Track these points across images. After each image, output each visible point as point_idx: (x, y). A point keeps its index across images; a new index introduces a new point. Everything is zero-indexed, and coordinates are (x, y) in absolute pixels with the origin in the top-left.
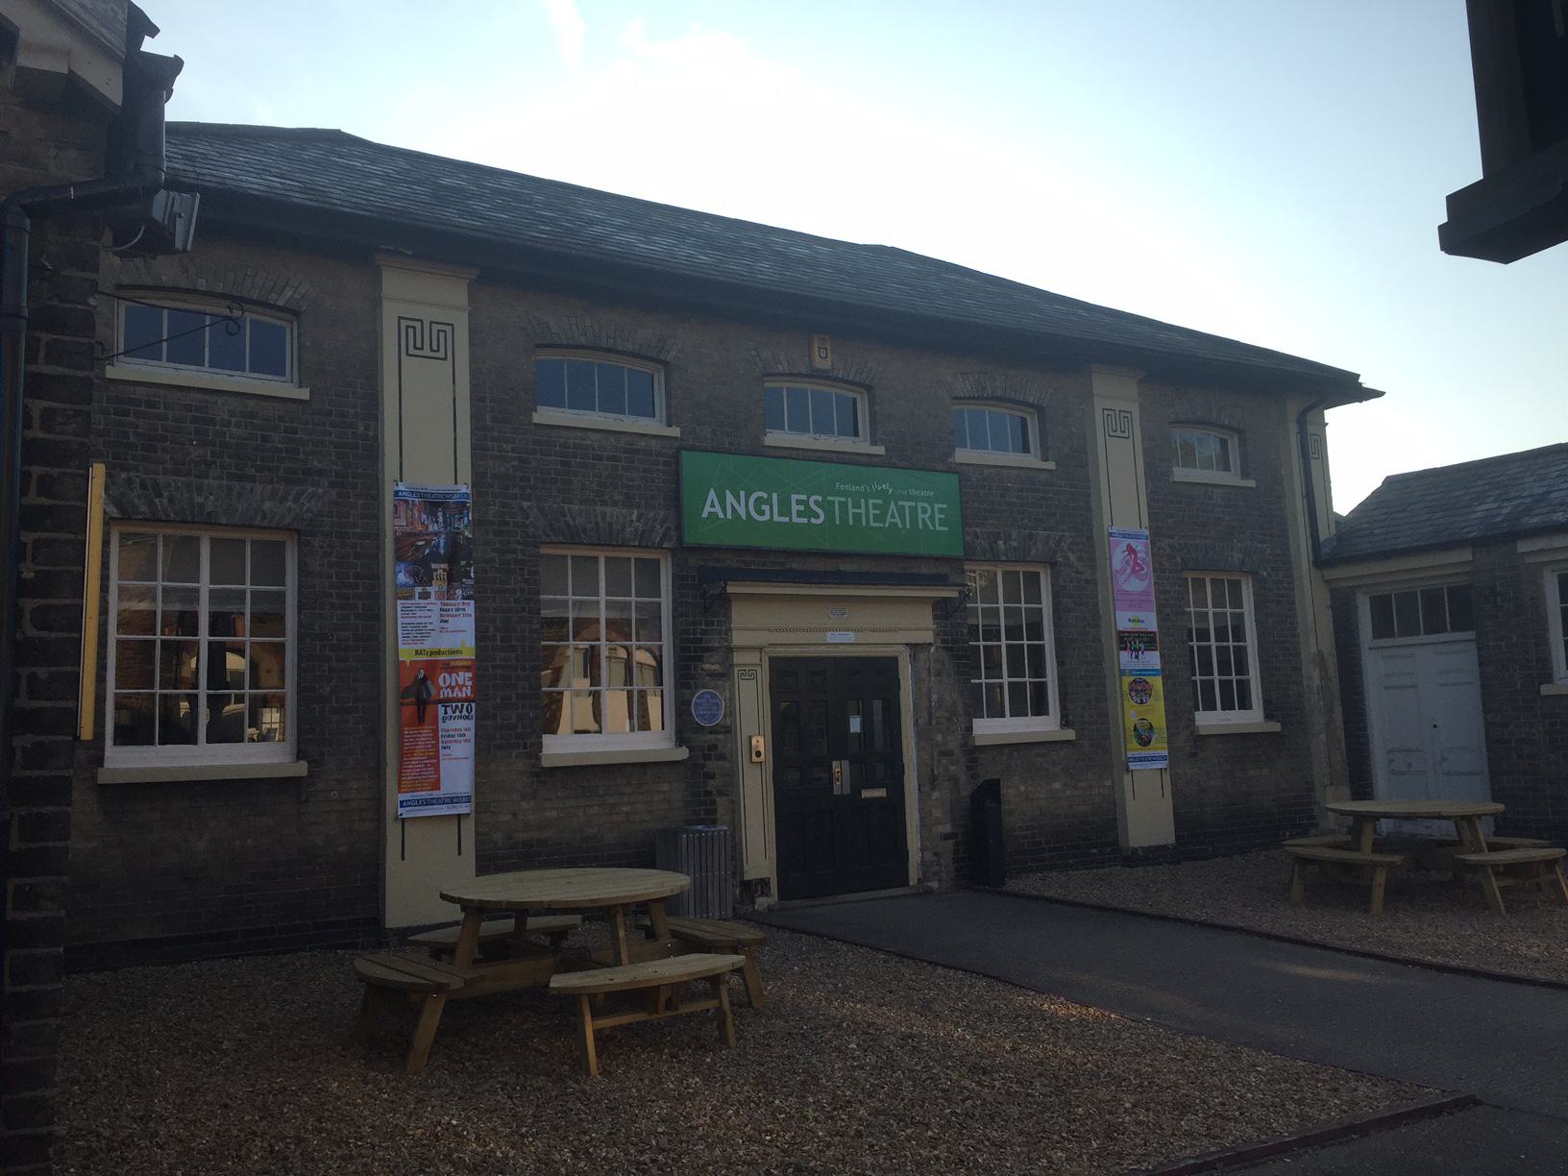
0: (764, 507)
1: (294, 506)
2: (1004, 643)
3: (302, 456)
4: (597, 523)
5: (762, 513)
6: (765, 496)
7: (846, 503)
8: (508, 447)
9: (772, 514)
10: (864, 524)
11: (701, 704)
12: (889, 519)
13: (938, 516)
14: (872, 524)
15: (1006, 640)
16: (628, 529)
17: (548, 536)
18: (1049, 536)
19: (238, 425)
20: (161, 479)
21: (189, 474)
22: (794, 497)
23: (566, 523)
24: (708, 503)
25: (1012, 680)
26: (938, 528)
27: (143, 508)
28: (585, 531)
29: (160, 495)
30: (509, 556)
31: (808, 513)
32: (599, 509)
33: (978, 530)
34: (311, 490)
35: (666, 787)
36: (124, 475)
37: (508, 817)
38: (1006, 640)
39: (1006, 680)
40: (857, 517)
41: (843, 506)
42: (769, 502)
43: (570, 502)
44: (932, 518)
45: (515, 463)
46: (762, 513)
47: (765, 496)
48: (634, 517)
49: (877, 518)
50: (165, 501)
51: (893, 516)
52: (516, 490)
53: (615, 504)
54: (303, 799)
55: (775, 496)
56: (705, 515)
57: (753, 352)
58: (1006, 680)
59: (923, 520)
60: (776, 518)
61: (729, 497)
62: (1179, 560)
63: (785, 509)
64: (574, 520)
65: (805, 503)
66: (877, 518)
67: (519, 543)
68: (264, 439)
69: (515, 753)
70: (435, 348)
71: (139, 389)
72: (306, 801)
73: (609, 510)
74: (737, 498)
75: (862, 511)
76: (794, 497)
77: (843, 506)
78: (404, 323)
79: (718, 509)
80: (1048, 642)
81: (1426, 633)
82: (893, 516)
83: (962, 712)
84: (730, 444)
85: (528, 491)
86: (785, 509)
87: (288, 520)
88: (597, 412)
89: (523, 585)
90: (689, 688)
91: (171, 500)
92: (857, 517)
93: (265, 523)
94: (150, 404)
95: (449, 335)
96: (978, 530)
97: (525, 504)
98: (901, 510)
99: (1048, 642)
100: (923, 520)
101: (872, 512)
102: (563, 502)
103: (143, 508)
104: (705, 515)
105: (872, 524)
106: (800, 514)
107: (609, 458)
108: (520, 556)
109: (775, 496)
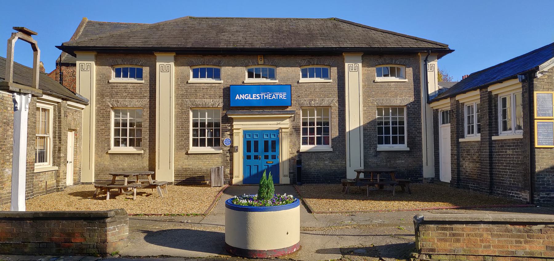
0: (247, 97)
1: (141, 103)
2: (316, 126)
3: (143, 94)
4: (202, 103)
5: (247, 98)
6: (248, 95)
7: (279, 95)
8: (183, 88)
9: (249, 98)
10: (267, 99)
11: (226, 141)
12: (273, 98)
13: (284, 96)
14: (269, 98)
15: (302, 126)
16: (210, 104)
17: (192, 106)
18: (329, 99)
19: (131, 89)
20: (119, 100)
21: (123, 98)
22: (254, 95)
23: (196, 103)
24: (237, 97)
25: (393, 135)
26: (284, 98)
27: (116, 105)
28: (200, 105)
29: (118, 103)
30: (183, 111)
31: (257, 97)
32: (203, 100)
33: (306, 99)
34: (144, 100)
35: (217, 158)
36: (113, 99)
37: (182, 163)
38: (302, 126)
39: (316, 136)
40: (266, 98)
41: (263, 96)
42: (249, 96)
43: (197, 99)
44: (283, 97)
45: (185, 91)
46: (247, 98)
47: (248, 95)
48: (211, 101)
49: (270, 97)
50: (119, 104)
51: (274, 97)
52: (185, 97)
53: (207, 98)
54: (143, 157)
55: (250, 95)
56: (236, 99)
57: (243, 61)
58: (316, 136)
59: (281, 97)
60: (250, 99)
61: (241, 95)
62: (376, 103)
63: (252, 97)
64: (197, 102)
65: (256, 96)
66: (270, 97)
67: (185, 108)
68: (136, 91)
69: (183, 150)
70: (82, 66)
71: (115, 84)
72: (143, 158)
73: (205, 100)
74: (242, 96)
75: (267, 96)
76: (254, 95)
77: (263, 96)
78: (161, 66)
79: (275, 97)
80: (405, 126)
81: (127, 127)
82: (274, 97)
83: (297, 144)
84: (236, 83)
85: (187, 97)
86: (252, 97)
87: (140, 106)
88: (129, 78)
89: (186, 117)
90: (223, 138)
91: (120, 103)
92: (266, 98)
93: (136, 107)
94: (117, 86)
95: (170, 67)
96: (306, 99)
97: (187, 100)
98: (276, 96)
99: (405, 126)
100: (281, 97)
101: (269, 96)
102: (195, 99)
103: (116, 105)
104: (236, 99)
105: (269, 98)
106: (255, 98)
107: (206, 89)
108: (185, 110)
109: (250, 95)
